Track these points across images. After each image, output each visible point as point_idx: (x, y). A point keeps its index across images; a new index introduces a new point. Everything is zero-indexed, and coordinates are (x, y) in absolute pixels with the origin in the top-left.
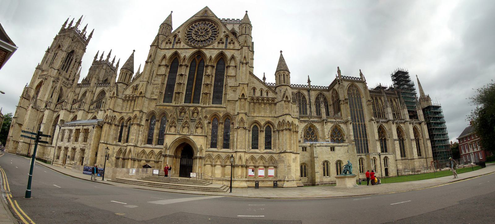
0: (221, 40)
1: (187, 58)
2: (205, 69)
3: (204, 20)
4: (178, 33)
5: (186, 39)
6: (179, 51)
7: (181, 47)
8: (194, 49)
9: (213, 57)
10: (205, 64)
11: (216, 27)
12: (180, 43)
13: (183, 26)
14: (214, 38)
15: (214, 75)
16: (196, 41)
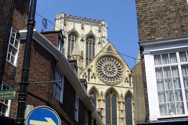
0: (127, 79)
1: (104, 93)
2: (117, 104)
3: (109, 56)
4: (91, 67)
5: (98, 74)
6: (97, 86)
7: (97, 83)
8: (108, 85)
9: (124, 94)
10: (117, 99)
11: (120, 64)
12: (95, 78)
13: (94, 60)
14: (120, 76)
15: (125, 110)
16: (107, 77)
